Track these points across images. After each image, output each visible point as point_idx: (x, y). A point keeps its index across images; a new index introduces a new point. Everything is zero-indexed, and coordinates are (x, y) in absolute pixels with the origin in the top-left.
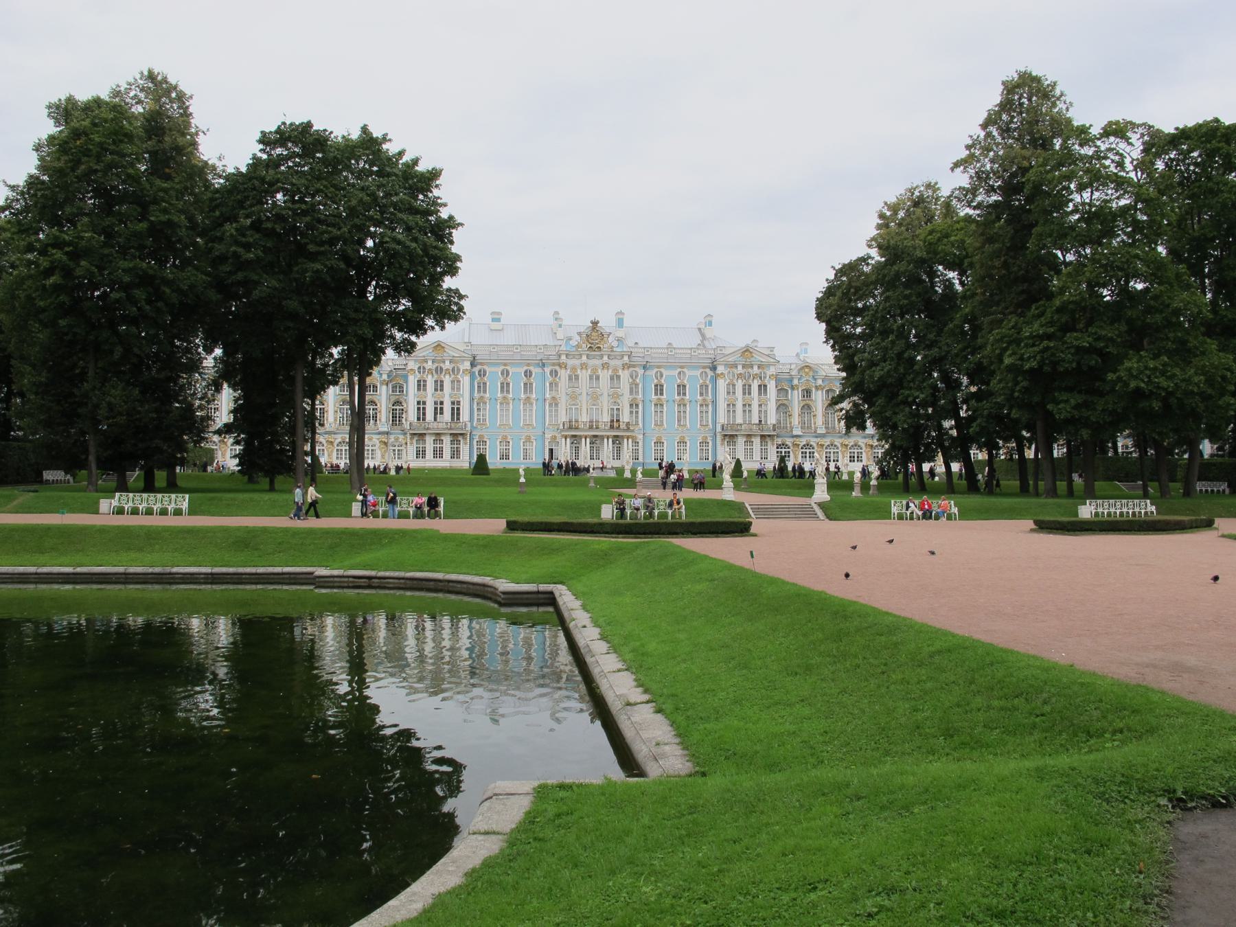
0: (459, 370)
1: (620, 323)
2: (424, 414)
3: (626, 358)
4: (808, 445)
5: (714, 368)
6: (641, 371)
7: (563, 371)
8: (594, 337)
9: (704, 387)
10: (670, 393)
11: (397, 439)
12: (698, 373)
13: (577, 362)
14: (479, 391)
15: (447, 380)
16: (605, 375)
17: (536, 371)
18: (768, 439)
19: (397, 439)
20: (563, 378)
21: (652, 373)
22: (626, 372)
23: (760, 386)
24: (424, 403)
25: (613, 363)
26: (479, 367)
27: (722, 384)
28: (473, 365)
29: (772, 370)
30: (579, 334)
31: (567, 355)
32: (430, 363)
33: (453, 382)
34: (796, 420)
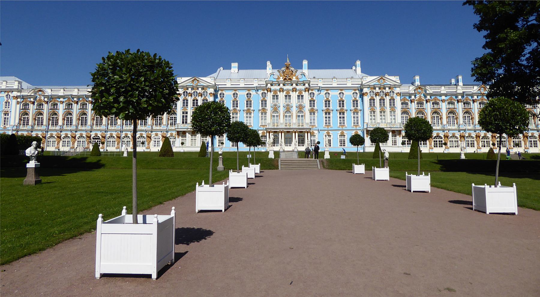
0: (207, 92)
2: (186, 120)
3: (307, 85)
5: (361, 90)
6: (316, 92)
9: (355, 102)
10: (334, 106)
12: (351, 93)
13: (278, 88)
16: (294, 95)
17: (253, 93)
24: (187, 113)
25: (298, 88)
27: (366, 99)
28: (216, 91)
31: (272, 85)
32: (190, 89)
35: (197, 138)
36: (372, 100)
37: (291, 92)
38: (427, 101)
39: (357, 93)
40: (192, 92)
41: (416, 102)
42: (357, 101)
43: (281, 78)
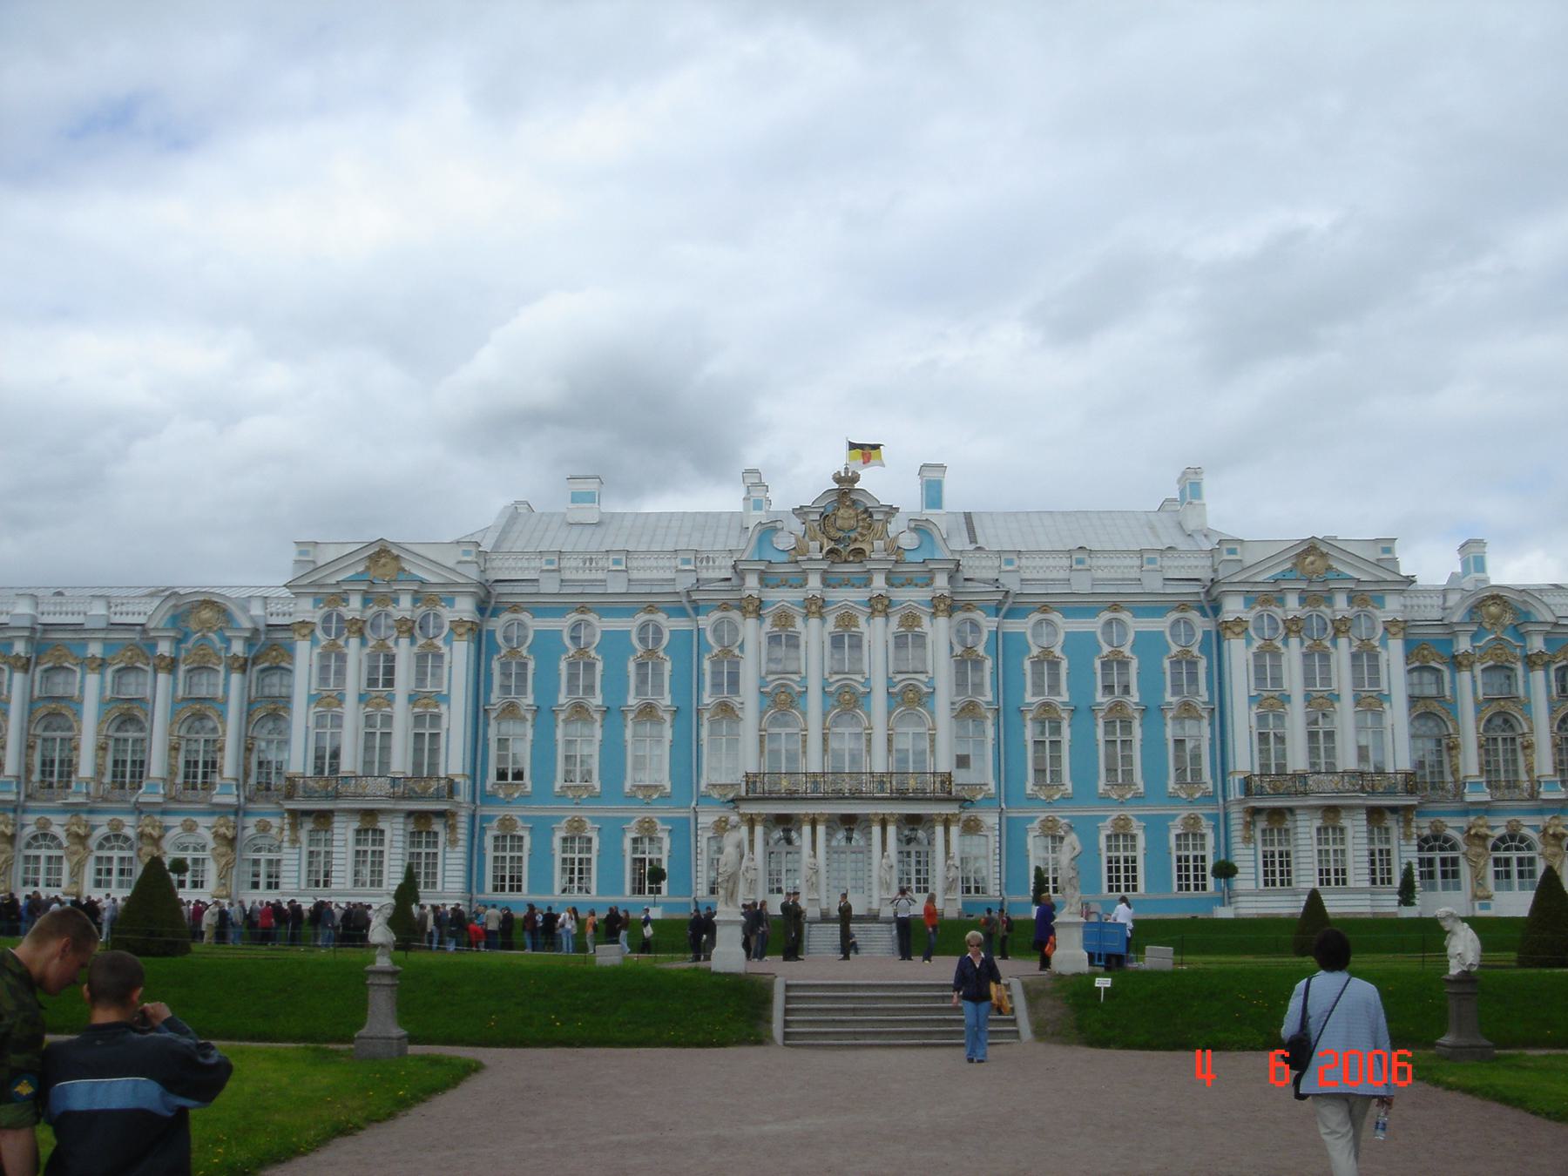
1: (933, 493)
3: (941, 581)
4: (1513, 839)
5: (1212, 606)
6: (988, 623)
7: (751, 623)
8: (845, 520)
11: (264, 828)
12: (1162, 624)
14: (505, 689)
15: (404, 653)
16: (876, 633)
17: (670, 625)
18: (1391, 822)
19: (264, 828)
20: (750, 647)
21: (1020, 626)
22: (942, 621)
23: (1355, 657)
26: (506, 617)
27: (1239, 654)
29: (1393, 607)
30: (801, 512)
31: (765, 579)
33: (421, 658)
34: (1470, 761)
35: (386, 848)
36: (1266, 661)
37: (862, 620)
38: (1530, 662)
39: (1187, 622)
40: (369, 613)
41: (1478, 668)
42: (1192, 664)
43: (814, 545)
